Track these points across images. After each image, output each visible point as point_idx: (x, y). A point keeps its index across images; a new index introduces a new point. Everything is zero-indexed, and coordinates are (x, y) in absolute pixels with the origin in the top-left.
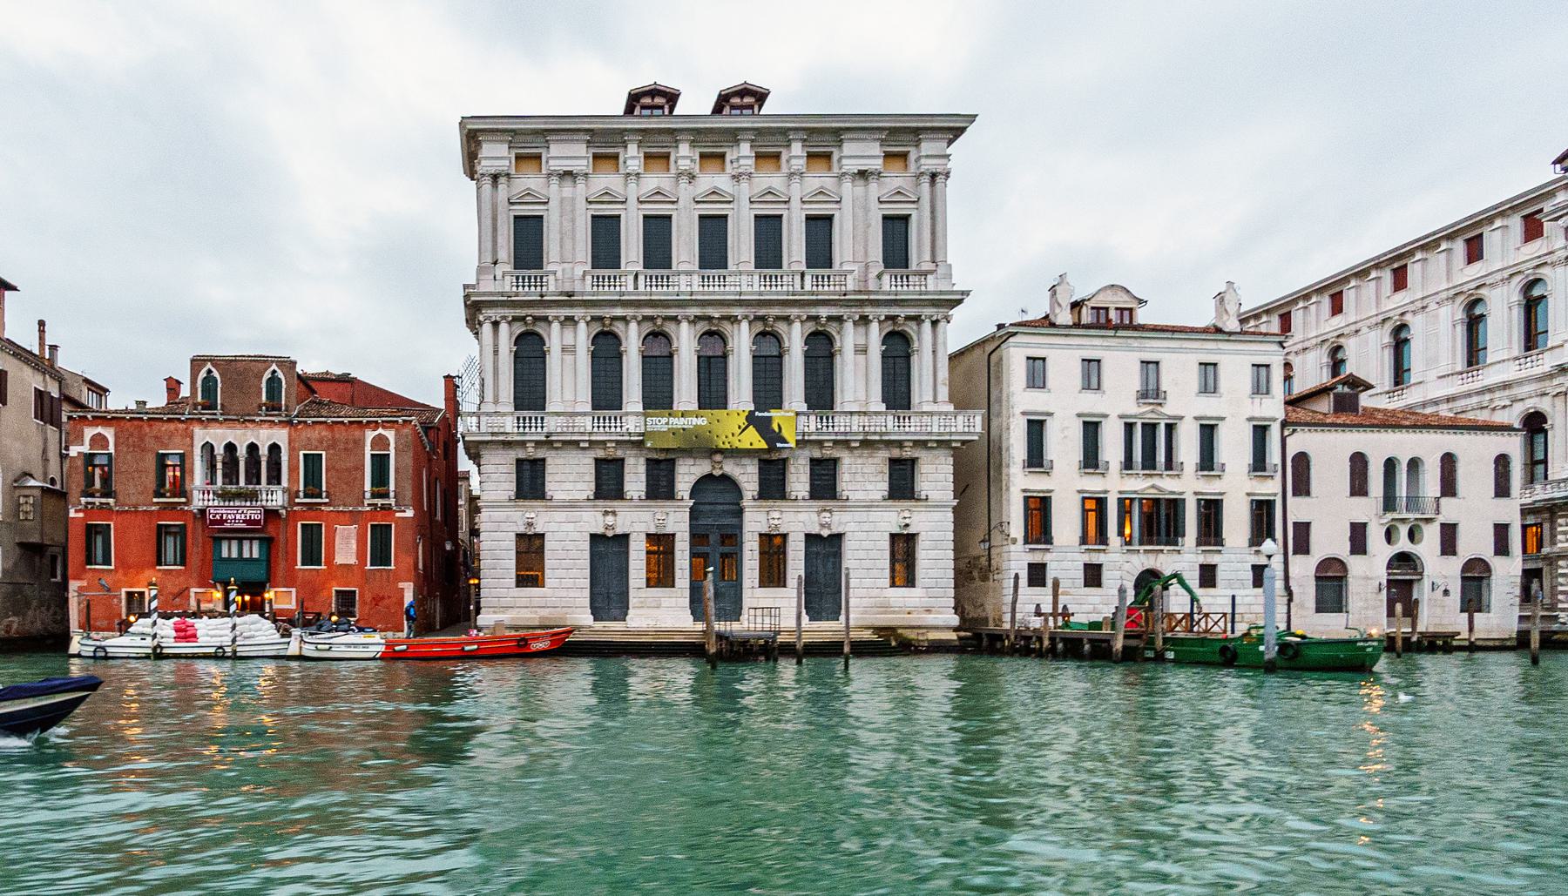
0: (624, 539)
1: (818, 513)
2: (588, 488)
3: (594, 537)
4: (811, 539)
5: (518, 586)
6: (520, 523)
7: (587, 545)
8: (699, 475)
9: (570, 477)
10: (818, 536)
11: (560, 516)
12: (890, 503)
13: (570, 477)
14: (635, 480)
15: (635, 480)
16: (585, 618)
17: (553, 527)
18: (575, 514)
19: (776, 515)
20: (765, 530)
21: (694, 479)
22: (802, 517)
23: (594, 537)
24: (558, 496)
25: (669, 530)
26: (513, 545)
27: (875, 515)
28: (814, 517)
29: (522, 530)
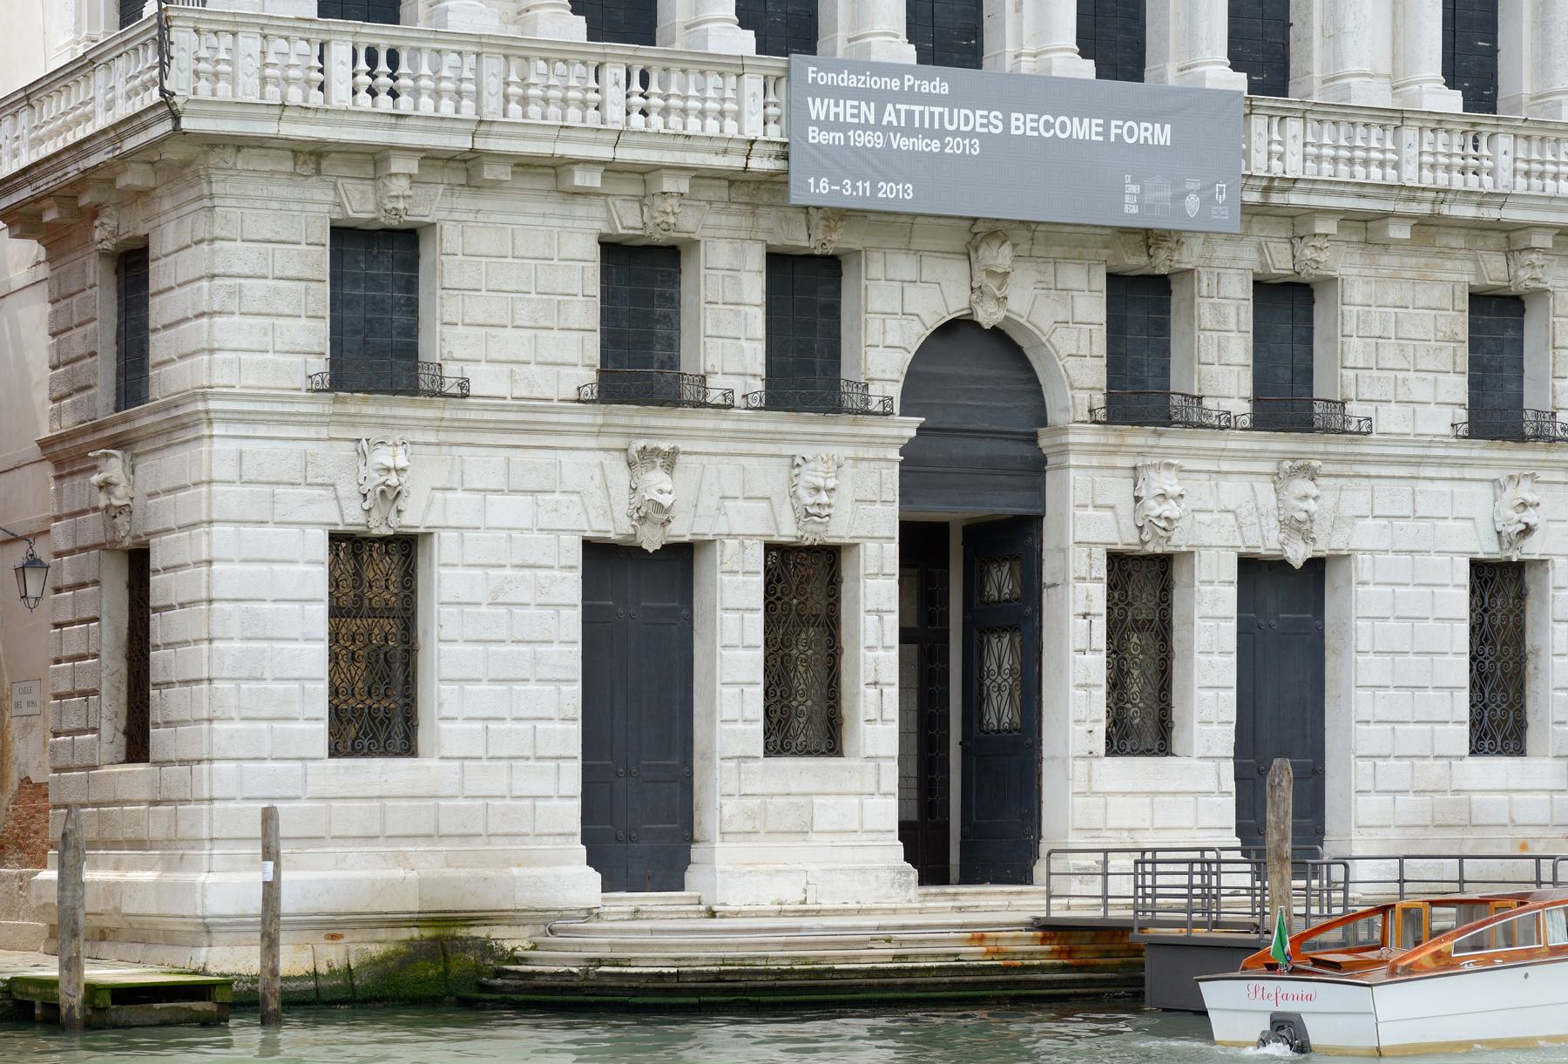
0: (682, 558)
1: (1278, 478)
2: (577, 353)
3: (598, 553)
4: (1256, 572)
5: (335, 752)
6: (347, 489)
7: (571, 587)
8: (934, 323)
9: (512, 304)
10: (1281, 565)
11: (485, 465)
12: (1480, 450)
13: (512, 304)
14: (727, 329)
15: (727, 329)
16: (573, 881)
17: (460, 508)
18: (532, 463)
19: (1168, 482)
20: (1126, 540)
21: (914, 335)
22: (1234, 492)
23: (598, 553)
24: (484, 381)
25: (835, 533)
26: (316, 580)
27: (1435, 494)
28: (1265, 489)
29: (353, 517)
